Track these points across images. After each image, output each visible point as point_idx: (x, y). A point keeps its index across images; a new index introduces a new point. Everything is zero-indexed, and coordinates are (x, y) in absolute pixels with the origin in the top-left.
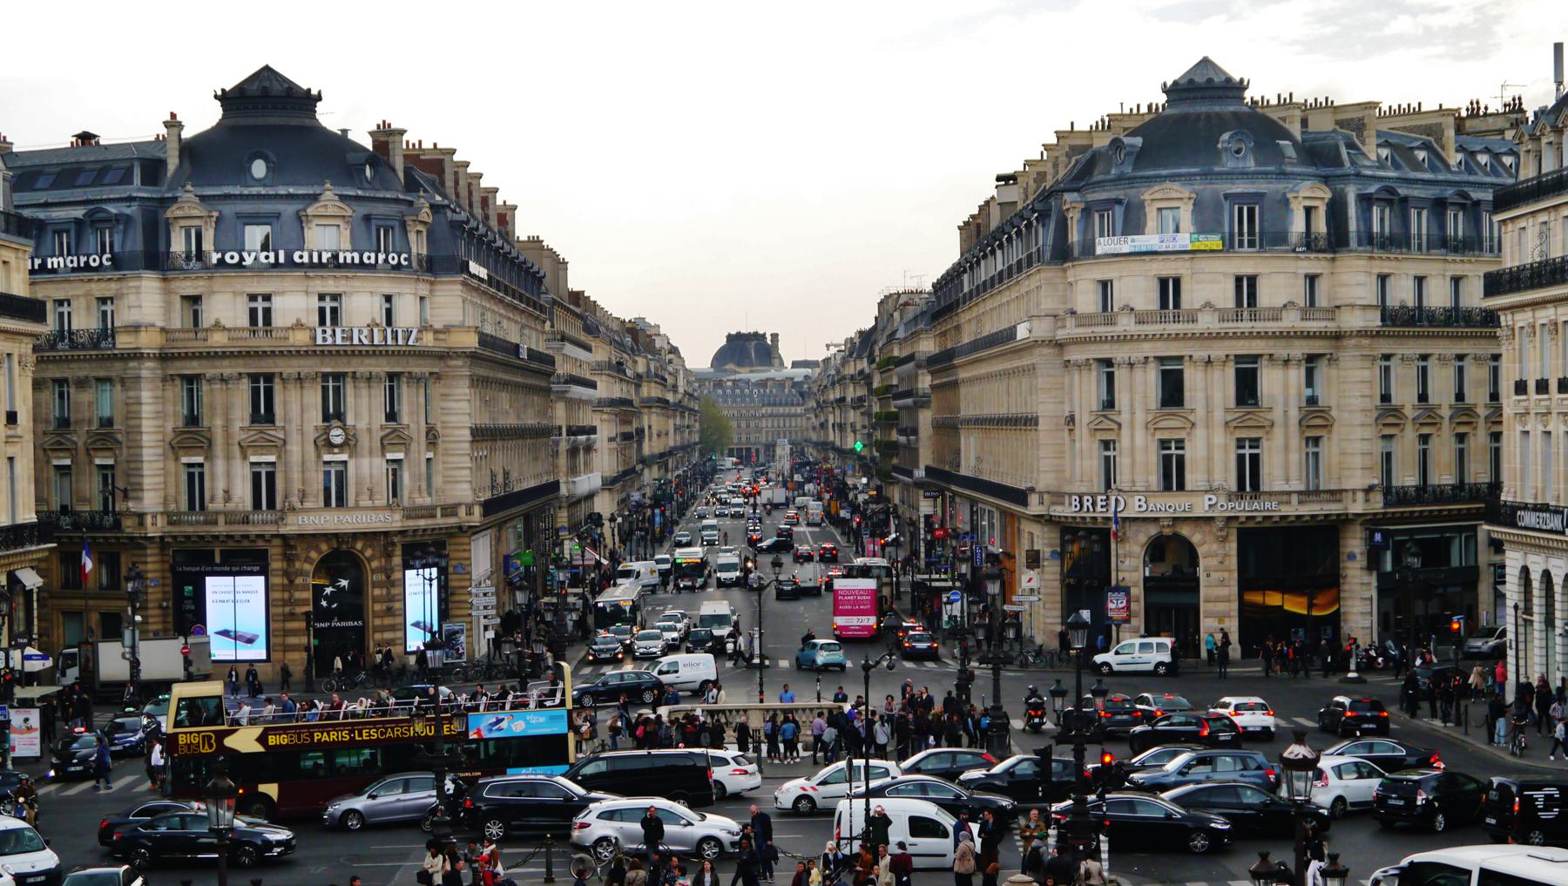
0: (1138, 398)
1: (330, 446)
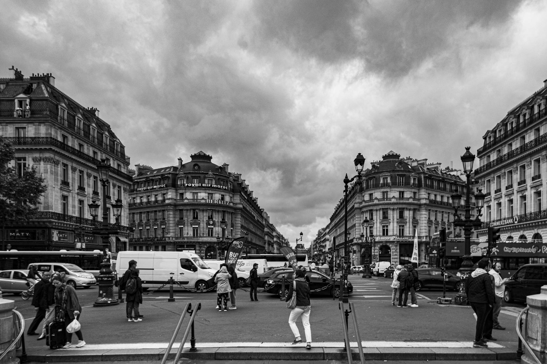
1: (210, 225)
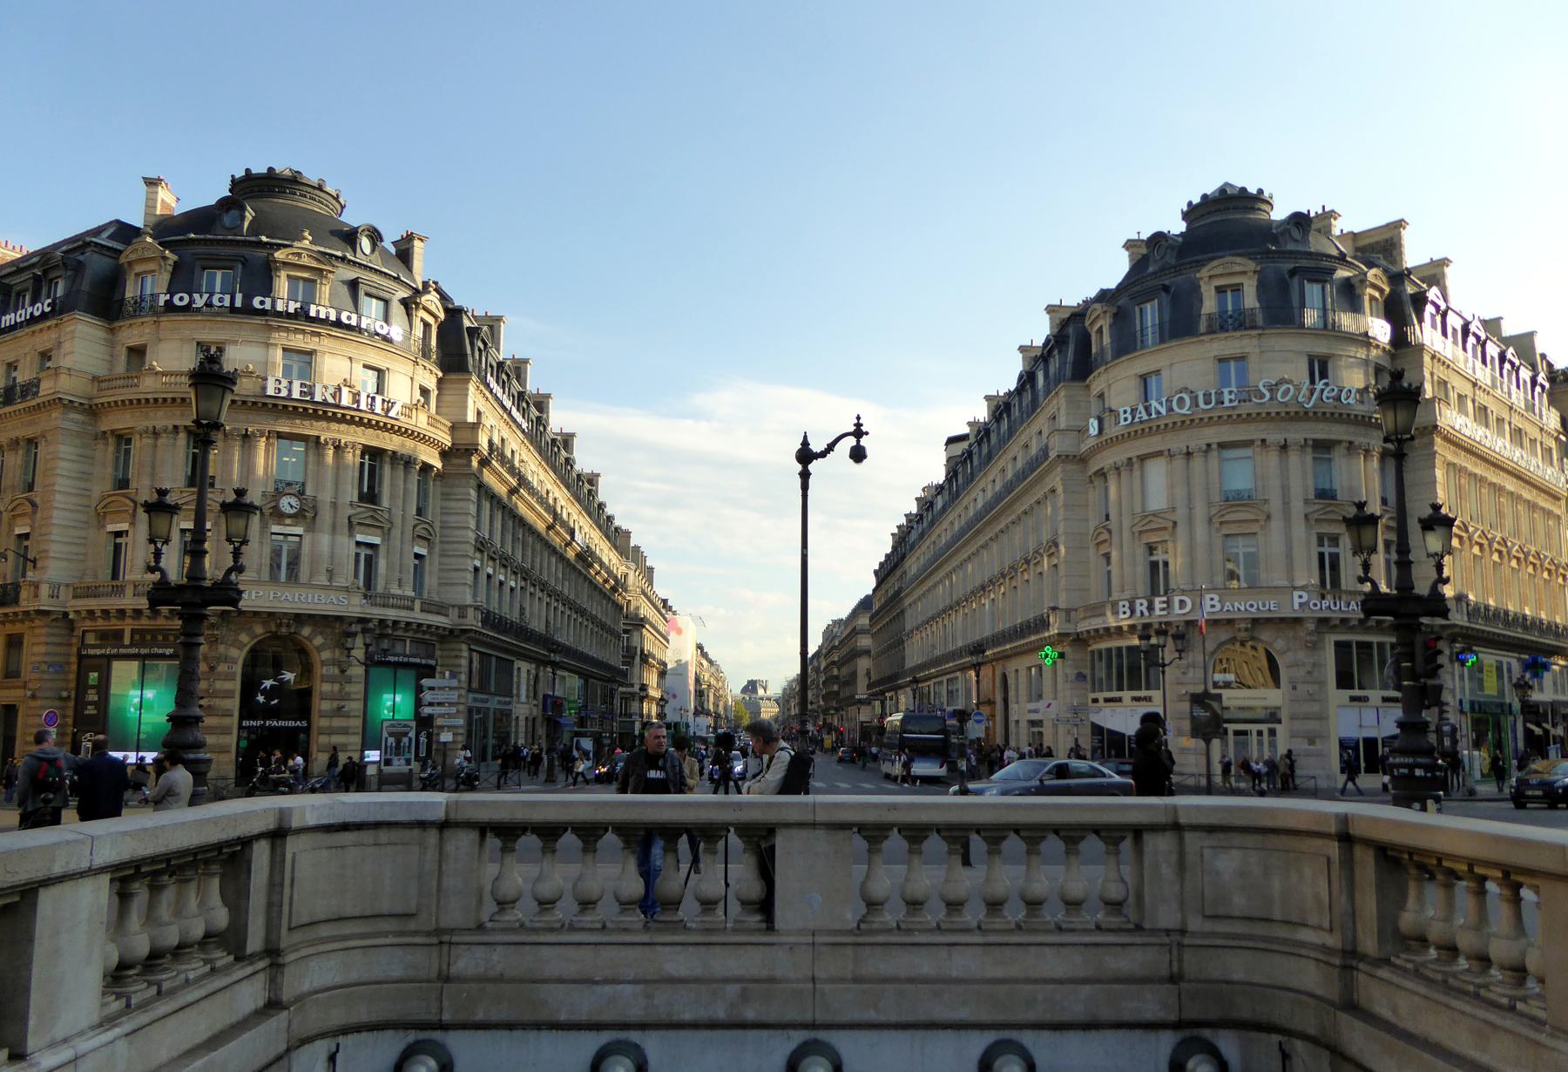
0: (1198, 490)
